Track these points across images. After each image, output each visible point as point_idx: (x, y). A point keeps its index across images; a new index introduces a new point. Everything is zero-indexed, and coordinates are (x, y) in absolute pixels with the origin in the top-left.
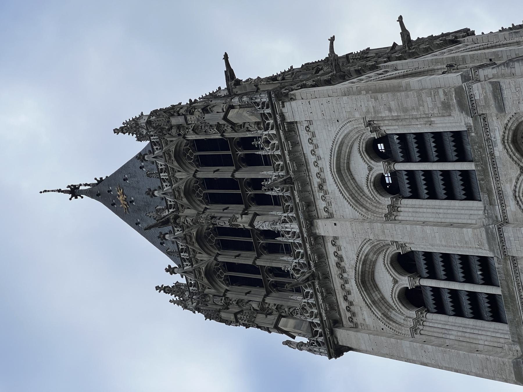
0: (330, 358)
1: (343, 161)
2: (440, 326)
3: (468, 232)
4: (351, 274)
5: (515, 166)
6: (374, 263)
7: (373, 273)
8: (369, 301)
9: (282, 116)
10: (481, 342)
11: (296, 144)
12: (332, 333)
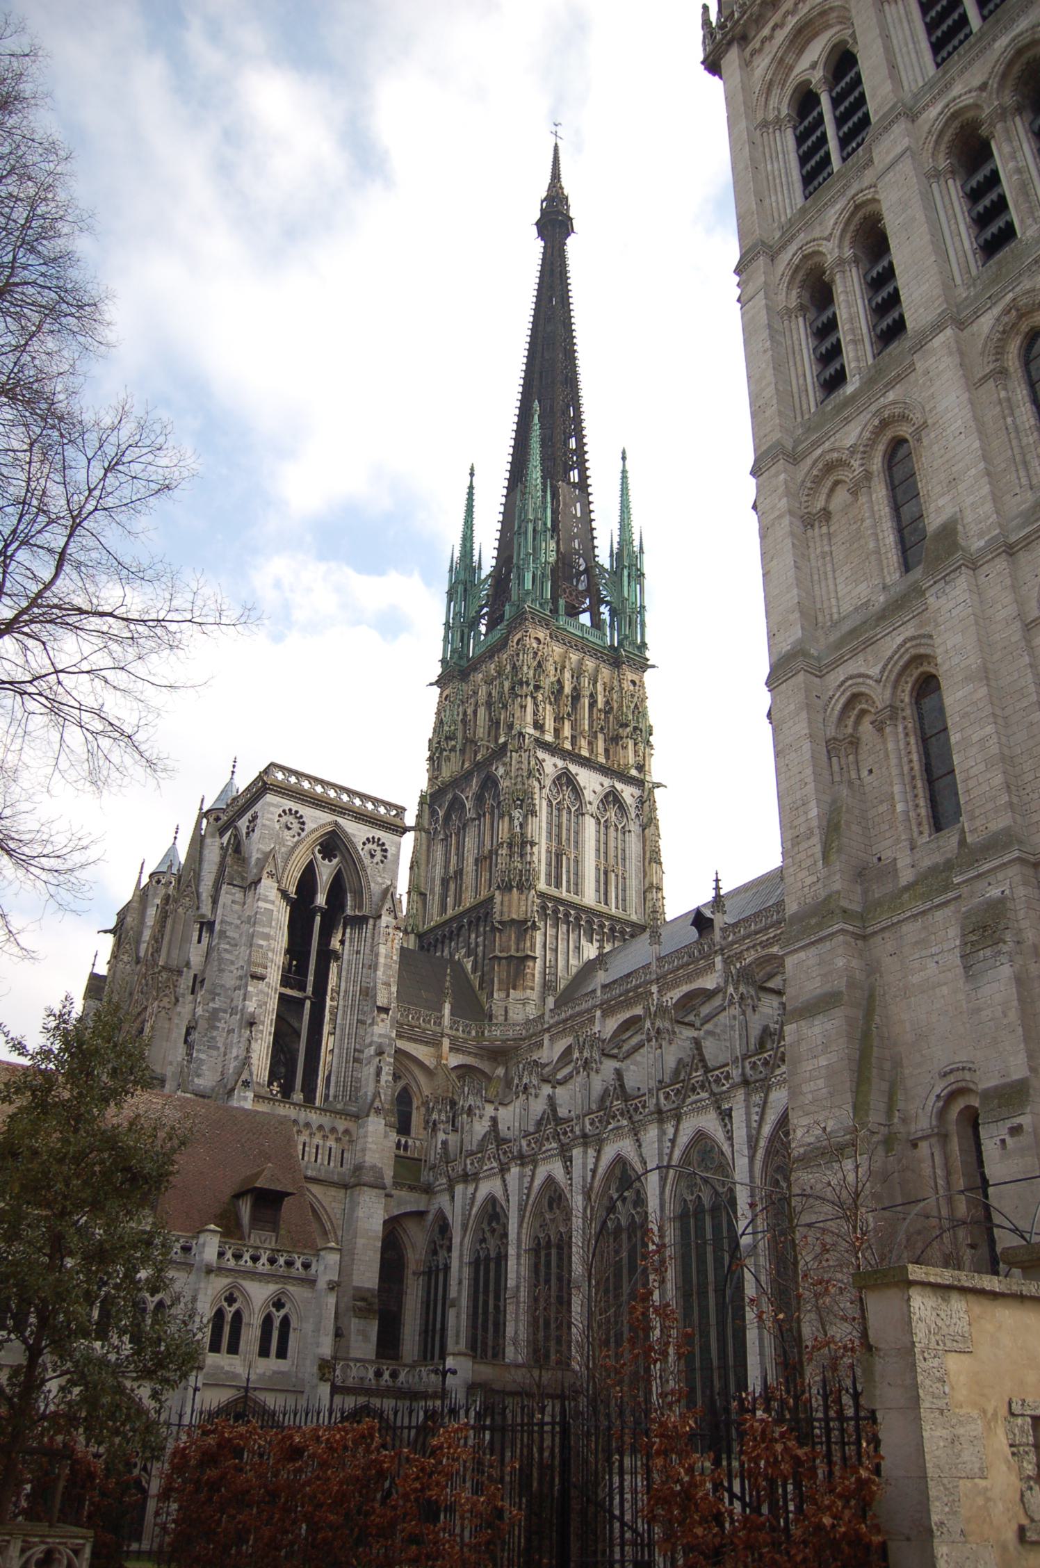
0: (703, 63)
2: (779, 148)
3: (888, 87)
5: (986, 76)
6: (828, 26)
8: (779, 55)
10: (773, 198)
12: (730, 44)
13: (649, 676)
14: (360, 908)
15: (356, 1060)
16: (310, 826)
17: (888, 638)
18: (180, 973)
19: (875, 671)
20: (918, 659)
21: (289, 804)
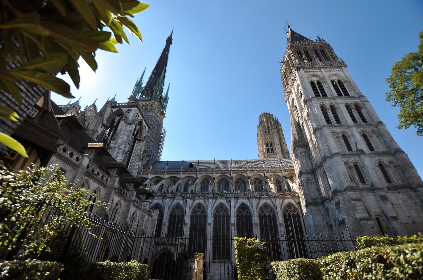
1: (338, 76)
4: (315, 73)
11: (337, 68)
12: (302, 68)
13: (164, 118)
14: (140, 138)
15: (133, 168)
16: (139, 118)
18: (95, 133)
21: (138, 112)
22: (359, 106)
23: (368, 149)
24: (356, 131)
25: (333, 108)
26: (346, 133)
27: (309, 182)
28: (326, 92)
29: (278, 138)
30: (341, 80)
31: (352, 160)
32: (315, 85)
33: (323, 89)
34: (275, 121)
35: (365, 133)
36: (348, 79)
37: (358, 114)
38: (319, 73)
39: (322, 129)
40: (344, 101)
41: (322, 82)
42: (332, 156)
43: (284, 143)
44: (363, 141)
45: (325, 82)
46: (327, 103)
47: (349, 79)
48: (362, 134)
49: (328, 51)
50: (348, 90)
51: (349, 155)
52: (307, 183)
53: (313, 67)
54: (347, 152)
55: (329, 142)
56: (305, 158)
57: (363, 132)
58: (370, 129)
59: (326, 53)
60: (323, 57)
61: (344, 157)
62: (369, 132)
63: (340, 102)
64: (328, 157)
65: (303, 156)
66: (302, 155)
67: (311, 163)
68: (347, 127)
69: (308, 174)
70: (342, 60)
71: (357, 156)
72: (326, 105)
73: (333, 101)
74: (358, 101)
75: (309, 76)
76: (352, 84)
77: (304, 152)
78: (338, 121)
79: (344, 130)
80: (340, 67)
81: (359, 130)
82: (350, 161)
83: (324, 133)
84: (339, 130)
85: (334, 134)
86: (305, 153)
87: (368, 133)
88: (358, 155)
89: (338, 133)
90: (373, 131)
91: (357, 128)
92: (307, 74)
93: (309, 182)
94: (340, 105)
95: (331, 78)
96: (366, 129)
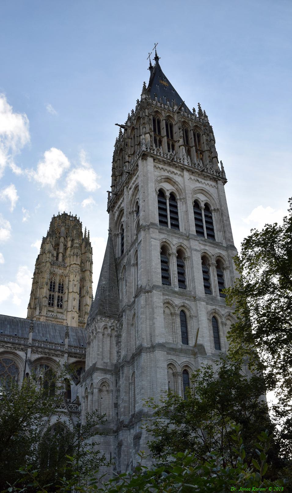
1: (208, 196)
4: (172, 176)
6: (173, 186)
7: (169, 183)
9: (219, 180)
11: (211, 179)
12: (152, 157)
17: (182, 357)
19: (179, 363)
20: (187, 366)
22: (223, 264)
23: (213, 345)
24: (203, 309)
25: (180, 254)
26: (189, 310)
27: (104, 388)
28: (180, 220)
29: (78, 278)
30: (211, 205)
31: (181, 360)
32: (166, 200)
33: (177, 213)
34: (83, 239)
35: (217, 316)
36: (221, 206)
37: (216, 278)
38: (178, 179)
39: (151, 291)
40: (202, 247)
41: (178, 197)
42: (153, 348)
43: (87, 292)
44: (209, 330)
45: (183, 199)
46: (174, 243)
47: (223, 208)
48: (212, 316)
49: (207, 140)
50: (215, 228)
51: (181, 351)
52: (100, 391)
53: (172, 163)
54: (178, 345)
55: (155, 320)
56: (109, 339)
57: (214, 314)
58: (226, 310)
59: (202, 142)
60: (194, 148)
61: (172, 352)
62: (223, 315)
63: (195, 247)
64: (147, 348)
65: (108, 334)
66: (106, 333)
67: (118, 352)
68: (192, 298)
69: (105, 374)
70: (222, 167)
71: (192, 356)
72: (171, 245)
73: (185, 242)
74: (224, 253)
75: (159, 179)
76: (225, 218)
77: (110, 327)
78: (182, 282)
79: (187, 302)
80: (215, 180)
81: (210, 307)
82: (179, 363)
83: (151, 301)
84: (177, 301)
85: (169, 306)
86: (113, 329)
87: (221, 317)
88: (195, 354)
89: (176, 305)
90: (229, 315)
91: (207, 304)
92: (158, 173)
93: (104, 388)
94: (194, 252)
95: (195, 196)
96: (220, 309)
